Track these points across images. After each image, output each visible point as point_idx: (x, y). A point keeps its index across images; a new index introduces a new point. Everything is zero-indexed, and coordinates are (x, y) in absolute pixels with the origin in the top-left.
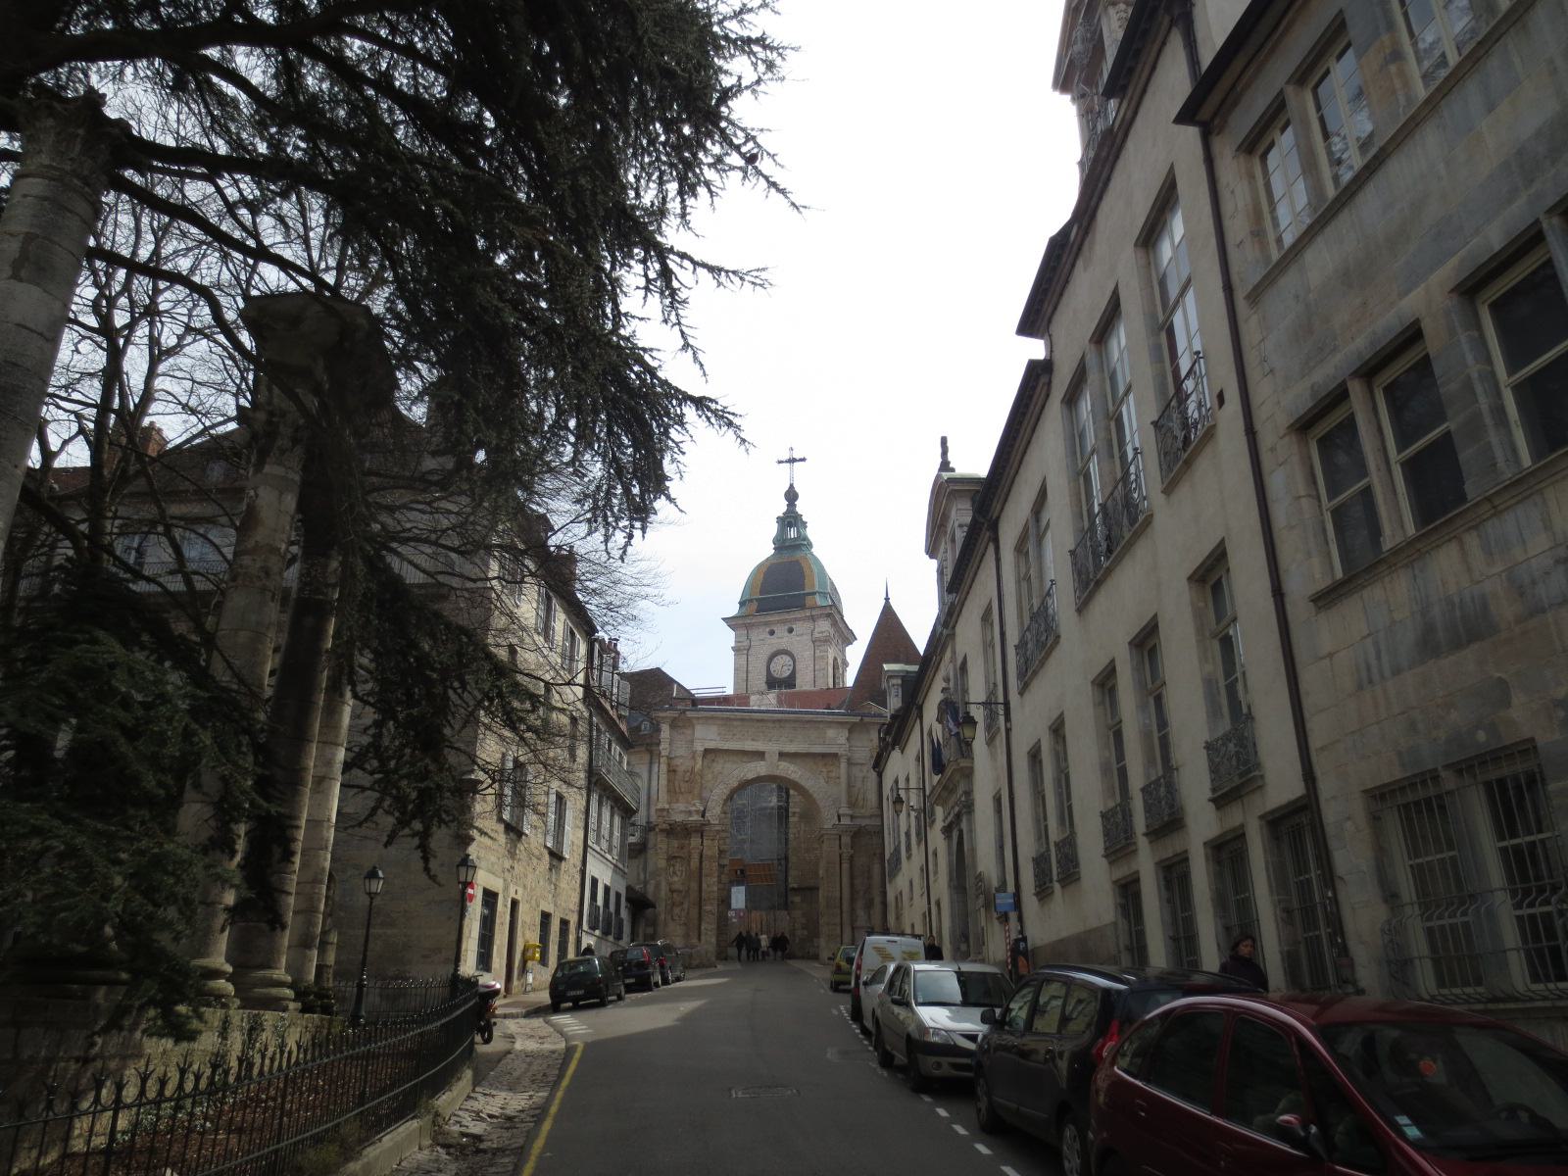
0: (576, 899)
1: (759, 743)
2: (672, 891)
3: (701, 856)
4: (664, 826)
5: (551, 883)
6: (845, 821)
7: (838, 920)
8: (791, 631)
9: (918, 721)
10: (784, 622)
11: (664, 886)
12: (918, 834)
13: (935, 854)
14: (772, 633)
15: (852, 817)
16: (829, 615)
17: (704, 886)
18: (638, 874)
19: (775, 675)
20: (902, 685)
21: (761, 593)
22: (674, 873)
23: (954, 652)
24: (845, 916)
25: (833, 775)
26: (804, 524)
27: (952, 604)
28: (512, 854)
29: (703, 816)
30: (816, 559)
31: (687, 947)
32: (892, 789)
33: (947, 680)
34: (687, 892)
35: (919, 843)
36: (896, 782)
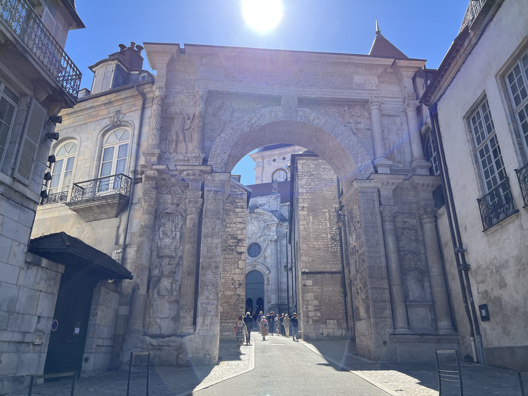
7: (386, 295)
18: (118, 237)
24: (396, 289)
25: (361, 126)
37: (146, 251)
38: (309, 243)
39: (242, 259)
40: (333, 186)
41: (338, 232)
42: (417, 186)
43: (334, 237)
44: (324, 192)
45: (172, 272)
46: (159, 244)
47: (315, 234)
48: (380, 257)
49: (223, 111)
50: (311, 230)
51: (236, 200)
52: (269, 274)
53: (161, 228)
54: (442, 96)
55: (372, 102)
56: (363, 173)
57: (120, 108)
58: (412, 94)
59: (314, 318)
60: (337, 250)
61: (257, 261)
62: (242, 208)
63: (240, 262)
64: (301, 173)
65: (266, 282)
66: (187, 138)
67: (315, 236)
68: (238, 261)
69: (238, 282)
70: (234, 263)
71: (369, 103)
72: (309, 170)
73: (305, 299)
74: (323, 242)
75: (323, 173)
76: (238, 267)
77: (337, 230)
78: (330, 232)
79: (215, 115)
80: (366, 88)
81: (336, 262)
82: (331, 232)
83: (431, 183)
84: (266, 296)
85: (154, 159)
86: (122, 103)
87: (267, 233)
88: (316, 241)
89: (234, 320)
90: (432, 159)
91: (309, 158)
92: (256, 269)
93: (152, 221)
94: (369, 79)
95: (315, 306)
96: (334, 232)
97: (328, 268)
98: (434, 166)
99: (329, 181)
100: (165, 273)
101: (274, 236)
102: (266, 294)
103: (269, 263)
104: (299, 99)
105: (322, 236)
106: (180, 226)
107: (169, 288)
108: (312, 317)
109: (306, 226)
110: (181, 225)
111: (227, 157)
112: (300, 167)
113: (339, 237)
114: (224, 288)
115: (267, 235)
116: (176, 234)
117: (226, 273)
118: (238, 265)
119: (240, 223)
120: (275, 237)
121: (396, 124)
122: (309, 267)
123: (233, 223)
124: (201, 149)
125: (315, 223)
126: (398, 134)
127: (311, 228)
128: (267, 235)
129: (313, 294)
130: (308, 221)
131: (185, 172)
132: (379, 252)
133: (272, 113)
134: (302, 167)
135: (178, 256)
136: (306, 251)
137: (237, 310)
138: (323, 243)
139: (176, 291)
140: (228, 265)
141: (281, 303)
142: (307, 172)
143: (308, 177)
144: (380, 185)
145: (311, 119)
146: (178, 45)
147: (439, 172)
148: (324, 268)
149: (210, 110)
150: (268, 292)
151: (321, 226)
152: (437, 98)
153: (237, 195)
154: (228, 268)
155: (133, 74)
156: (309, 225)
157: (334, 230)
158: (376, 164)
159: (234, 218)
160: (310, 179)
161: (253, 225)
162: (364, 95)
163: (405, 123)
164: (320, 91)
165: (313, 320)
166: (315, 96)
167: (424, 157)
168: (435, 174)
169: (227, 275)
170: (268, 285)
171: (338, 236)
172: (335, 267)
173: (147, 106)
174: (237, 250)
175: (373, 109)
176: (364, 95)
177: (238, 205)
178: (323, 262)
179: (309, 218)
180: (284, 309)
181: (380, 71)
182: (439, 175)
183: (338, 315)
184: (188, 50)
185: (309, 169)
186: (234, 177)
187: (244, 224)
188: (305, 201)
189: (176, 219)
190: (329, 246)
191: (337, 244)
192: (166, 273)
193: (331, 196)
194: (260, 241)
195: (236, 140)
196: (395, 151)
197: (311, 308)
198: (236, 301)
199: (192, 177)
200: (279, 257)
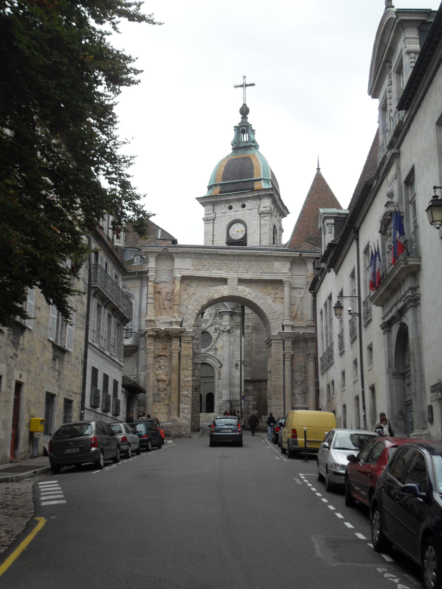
0: (79, 384)
2: (158, 381)
4: (152, 333)
5: (55, 370)
6: (288, 330)
7: (282, 403)
8: (244, 206)
9: (355, 243)
10: (239, 200)
11: (152, 378)
12: (352, 333)
13: (370, 348)
14: (230, 208)
15: (293, 327)
16: (271, 196)
17: (182, 376)
19: (232, 237)
20: (335, 224)
21: (223, 179)
22: (160, 367)
23: (399, 169)
24: (288, 400)
26: (253, 131)
27: (401, 122)
28: (16, 344)
29: (181, 326)
30: (261, 155)
31: (169, 421)
32: (325, 305)
33: (391, 195)
34: (170, 381)
35: (353, 341)
36: (330, 298)
46: (157, 373)
49: (190, 287)
50: (254, 346)
52: (220, 367)
56: (275, 330)
58: (311, 274)
61: (207, 353)
62: (198, 326)
65: (217, 376)
68: (195, 370)
79: (185, 290)
92: (206, 362)
95: (253, 405)
100: (161, 390)
102: (216, 389)
103: (220, 355)
105: (262, 350)
115: (218, 324)
118: (195, 373)
126: (301, 301)
128: (218, 324)
129: (252, 397)
130: (252, 338)
131: (171, 332)
139: (167, 399)
141: (233, 398)
144: (284, 339)
150: (218, 386)
151: (262, 342)
173: (143, 285)
176: (280, 277)
180: (236, 405)
181: (292, 259)
194: (211, 330)
196: (298, 313)
197: (251, 407)
199: (175, 335)
200: (232, 349)
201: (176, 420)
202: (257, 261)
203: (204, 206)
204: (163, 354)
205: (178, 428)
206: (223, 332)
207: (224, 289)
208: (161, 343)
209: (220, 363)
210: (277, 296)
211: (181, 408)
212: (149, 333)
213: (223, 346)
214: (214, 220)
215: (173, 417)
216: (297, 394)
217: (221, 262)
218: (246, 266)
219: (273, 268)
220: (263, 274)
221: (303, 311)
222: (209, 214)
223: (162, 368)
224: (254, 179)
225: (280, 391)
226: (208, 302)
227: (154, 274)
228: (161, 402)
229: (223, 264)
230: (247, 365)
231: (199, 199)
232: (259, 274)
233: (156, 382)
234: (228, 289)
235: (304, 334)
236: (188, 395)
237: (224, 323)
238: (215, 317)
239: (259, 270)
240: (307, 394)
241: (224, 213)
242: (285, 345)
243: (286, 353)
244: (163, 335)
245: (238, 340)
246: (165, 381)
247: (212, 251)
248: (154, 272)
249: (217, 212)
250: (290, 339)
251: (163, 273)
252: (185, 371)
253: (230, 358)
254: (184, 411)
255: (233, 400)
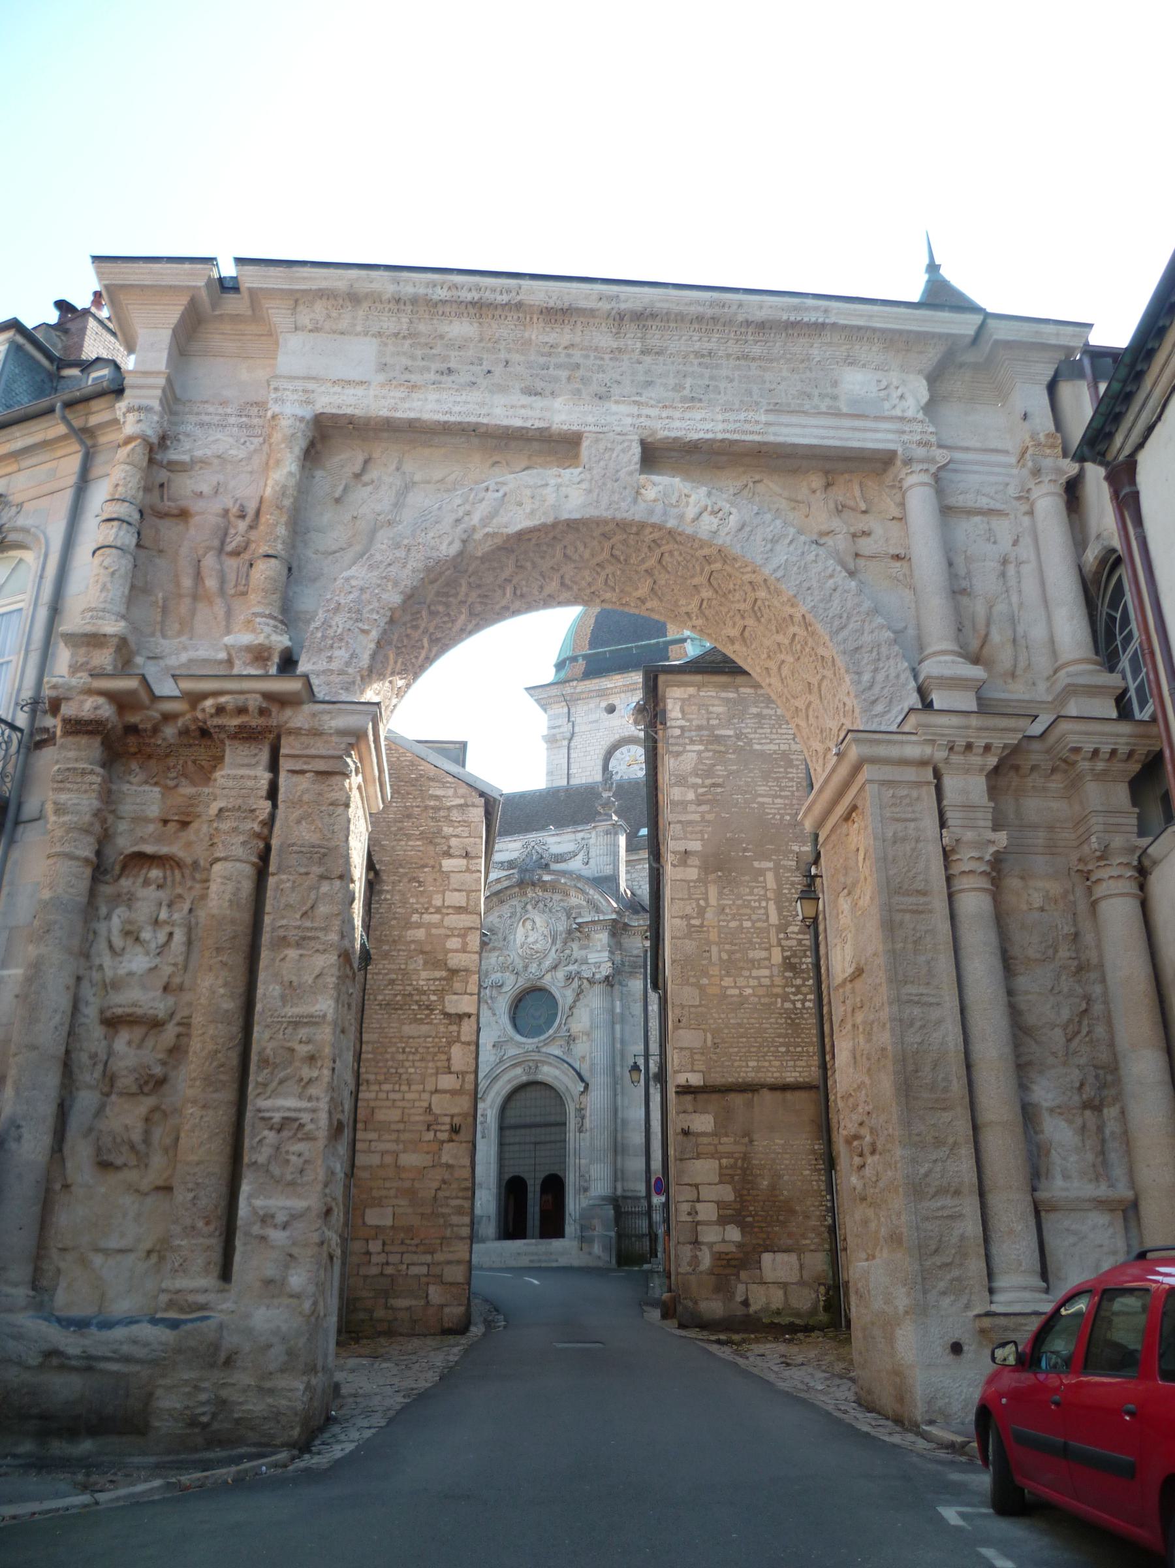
1: (558, 403)
2: (112, 1023)
3: (265, 856)
7: (964, 1167)
17: (268, 990)
21: (593, 643)
37: (56, 998)
38: (705, 981)
39: (463, 1039)
40: (792, 780)
41: (807, 943)
42: (1073, 757)
43: (793, 960)
44: (760, 799)
45: (152, 1076)
46: (109, 973)
47: (727, 951)
48: (939, 1022)
49: (369, 488)
50: (713, 936)
51: (445, 829)
52: (582, 1093)
53: (119, 911)
54: (1150, 429)
55: (908, 462)
56: (879, 708)
57: (8, 486)
58: (1047, 436)
59: (716, 1248)
60: (803, 1004)
61: (544, 1050)
62: (467, 855)
63: (456, 1051)
64: (677, 732)
66: (233, 583)
67: (725, 956)
68: (450, 1044)
69: (447, 1120)
70: (435, 1054)
71: (899, 463)
72: (705, 723)
73: (686, 1180)
74: (754, 978)
75: (755, 732)
76: (449, 1068)
77: (804, 934)
78: (779, 940)
80: (887, 413)
81: (799, 1049)
82: (784, 943)
83: (1123, 750)
84: (572, 1169)
85: (104, 658)
86: (14, 467)
87: (577, 953)
88: (728, 974)
89: (432, 1253)
90: (1125, 662)
91: (707, 678)
92: (540, 1077)
93: (84, 885)
94: (895, 383)
95: (720, 1204)
96: (794, 943)
97: (774, 1071)
98: (1132, 687)
99: (776, 759)
100: (120, 1083)
101: (603, 965)
102: (571, 1161)
103: (583, 1057)
104: (643, 443)
105: (751, 954)
106: (187, 907)
107: (136, 1136)
108: (711, 1245)
109: (693, 922)
110: (192, 903)
111: (372, 646)
112: (674, 710)
113: (809, 960)
114: (397, 1141)
115: (576, 961)
116: (171, 934)
117: (404, 1088)
118: (449, 1060)
119: (460, 910)
120: (606, 970)
121: (995, 543)
122: (703, 1068)
123: (432, 910)
124: (275, 618)
125: (727, 911)
126: (1003, 575)
127: (713, 927)
128: (576, 961)
130: (702, 903)
131: (209, 703)
132: (938, 1004)
133: (544, 492)
134: (682, 711)
135: (177, 1018)
136: (692, 1010)
137: (441, 1221)
138: (755, 983)
140: (413, 1061)
141: (624, 1190)
142: (700, 728)
143: (701, 748)
144: (941, 754)
145: (691, 512)
146: (210, 261)
147: (1149, 709)
148: (758, 1069)
149: (323, 480)
151: (750, 919)
152: (1135, 437)
153: (449, 809)
154: (412, 1070)
155: (69, 377)
156: (707, 915)
157: (793, 933)
158: (928, 677)
159: (437, 892)
160: (711, 754)
161: (529, 925)
162: (879, 436)
163: (1027, 540)
164: (720, 417)
165: (713, 1254)
166: (701, 435)
167: (1097, 653)
168: (1138, 716)
169: (408, 1096)
170: (580, 1132)
171: (806, 956)
172: (795, 1066)
174: (444, 1007)
175: (911, 487)
176: (879, 436)
177: (450, 847)
178: (753, 1049)
179: (706, 893)
180: (632, 1213)
182: (1154, 719)
183: (804, 1236)
184: (251, 279)
185: (708, 719)
186: (445, 749)
187: (470, 913)
188: (692, 833)
189: (173, 881)
190: (778, 990)
191: (803, 985)
192: (126, 1081)
193: (782, 816)
194: (554, 982)
195: (406, 586)
197: (707, 1212)
198: (439, 1189)
199: (236, 722)
200: (618, 1035)
201: (203, 1307)
202: (745, 357)
203: (544, 706)
204: (164, 850)
205: (212, 1366)
206: (591, 982)
207: (559, 486)
208: (156, 784)
209: (582, 1079)
210: (867, 546)
211: (243, 1211)
212: (67, 710)
213: (591, 1027)
214: (570, 740)
215: (182, 1283)
216: (1051, 1110)
217: (542, 360)
218: (689, 382)
219: (835, 398)
220: (785, 419)
221: (1020, 630)
222: (559, 727)
223: (146, 935)
224: (668, 638)
225: (946, 1090)
226: (461, 553)
227: (156, 404)
228: (118, 1168)
229: (558, 366)
230: (684, 1020)
231: (532, 692)
232: (763, 418)
233: (98, 1031)
234: (584, 486)
235: (1064, 726)
236: (305, 1117)
237: (593, 957)
238: (565, 943)
239: (757, 403)
240: (1111, 1112)
241: (596, 721)
242: (950, 797)
243: (957, 841)
244: (170, 731)
245: (638, 1009)
246: (155, 1024)
247: (494, 290)
248: (159, 392)
249: (579, 720)
250: (976, 760)
251: (216, 419)
252: (292, 953)
253: (614, 1066)
254: (263, 1238)
255: (625, 1198)
